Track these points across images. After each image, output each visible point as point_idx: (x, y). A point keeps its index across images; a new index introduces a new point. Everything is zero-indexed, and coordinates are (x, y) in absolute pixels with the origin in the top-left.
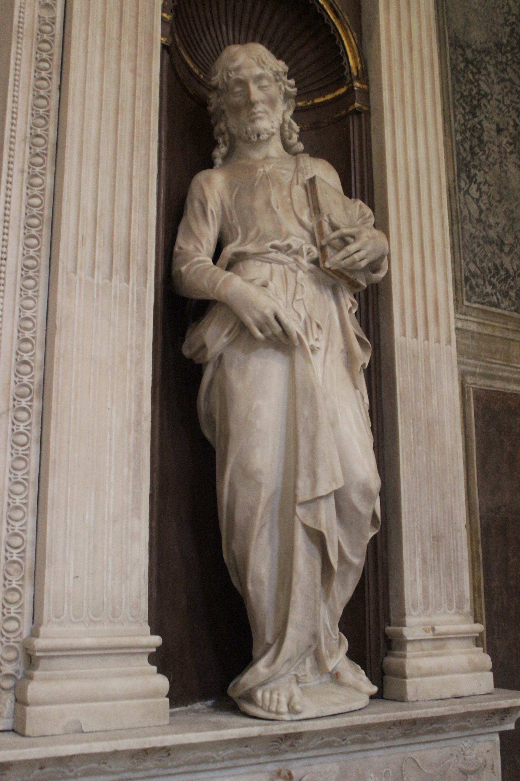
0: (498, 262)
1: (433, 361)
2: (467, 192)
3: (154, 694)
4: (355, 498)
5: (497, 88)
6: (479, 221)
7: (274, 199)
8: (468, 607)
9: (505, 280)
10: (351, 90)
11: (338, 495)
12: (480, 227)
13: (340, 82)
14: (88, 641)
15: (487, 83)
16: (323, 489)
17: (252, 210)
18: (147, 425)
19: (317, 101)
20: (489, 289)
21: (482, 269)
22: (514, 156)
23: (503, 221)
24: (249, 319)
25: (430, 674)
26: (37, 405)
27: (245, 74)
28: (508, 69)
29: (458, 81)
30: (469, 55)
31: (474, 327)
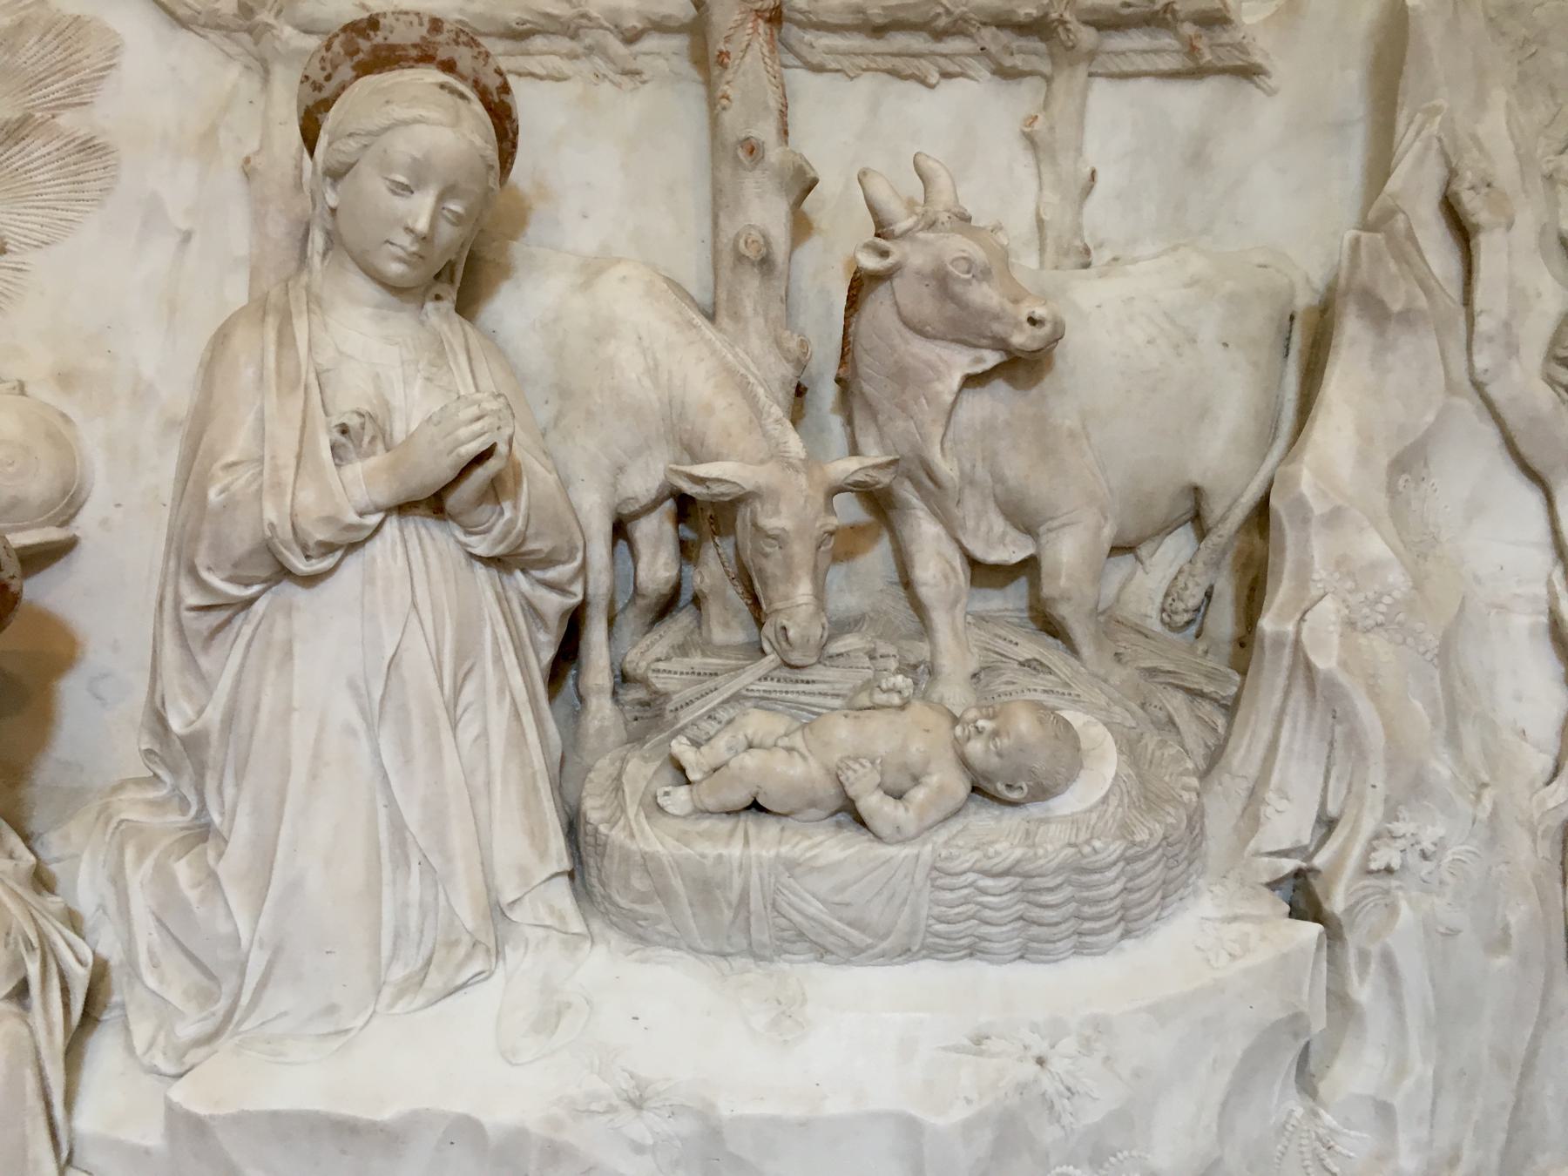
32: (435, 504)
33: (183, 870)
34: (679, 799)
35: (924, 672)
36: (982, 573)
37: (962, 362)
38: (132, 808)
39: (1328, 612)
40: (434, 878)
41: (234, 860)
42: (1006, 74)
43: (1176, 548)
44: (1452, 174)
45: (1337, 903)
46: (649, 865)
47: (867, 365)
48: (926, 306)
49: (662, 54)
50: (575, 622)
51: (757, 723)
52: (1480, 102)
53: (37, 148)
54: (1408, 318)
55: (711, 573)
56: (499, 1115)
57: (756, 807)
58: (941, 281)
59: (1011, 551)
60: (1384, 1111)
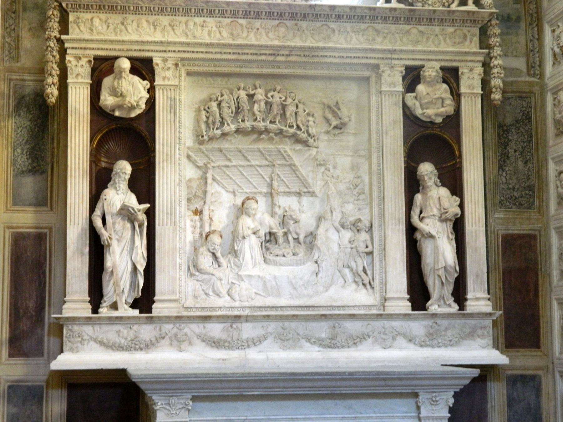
0: (512, 195)
1: (477, 232)
2: (502, 175)
3: (409, 306)
4: (449, 268)
5: (516, 137)
6: (505, 183)
7: (431, 203)
8: (487, 291)
9: (515, 200)
10: (456, 162)
11: (445, 268)
12: (506, 185)
13: (454, 159)
14: (395, 296)
15: (511, 136)
16: (440, 267)
17: (426, 206)
18: (405, 255)
19: (449, 164)
20: (508, 204)
21: (506, 199)
22: (521, 159)
23: (515, 181)
24: (424, 233)
25: (473, 306)
26: (383, 252)
27: (423, 174)
28: (521, 129)
29: (500, 139)
30: (505, 128)
31: (502, 216)
32: (254, 233)
33: (236, 260)
34: (271, 255)
35: (290, 246)
36: (294, 239)
37: (292, 222)
38: (229, 256)
39: (319, 242)
40: (255, 260)
41: (241, 259)
42: (296, 196)
43: (310, 237)
44: (331, 208)
45: (319, 262)
46: (270, 260)
47: (285, 222)
48: (289, 217)
49: (269, 195)
50: (262, 242)
51: (277, 250)
52: (334, 201)
53: (217, 203)
54: (327, 219)
55: (272, 238)
56: (261, 275)
57: (277, 256)
58: (291, 216)
59: (296, 237)
60: (322, 278)
